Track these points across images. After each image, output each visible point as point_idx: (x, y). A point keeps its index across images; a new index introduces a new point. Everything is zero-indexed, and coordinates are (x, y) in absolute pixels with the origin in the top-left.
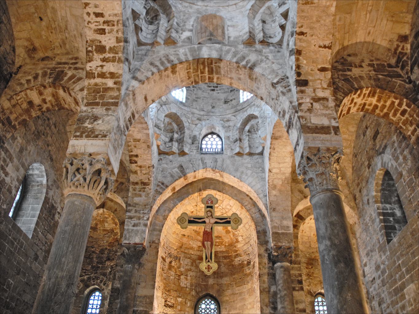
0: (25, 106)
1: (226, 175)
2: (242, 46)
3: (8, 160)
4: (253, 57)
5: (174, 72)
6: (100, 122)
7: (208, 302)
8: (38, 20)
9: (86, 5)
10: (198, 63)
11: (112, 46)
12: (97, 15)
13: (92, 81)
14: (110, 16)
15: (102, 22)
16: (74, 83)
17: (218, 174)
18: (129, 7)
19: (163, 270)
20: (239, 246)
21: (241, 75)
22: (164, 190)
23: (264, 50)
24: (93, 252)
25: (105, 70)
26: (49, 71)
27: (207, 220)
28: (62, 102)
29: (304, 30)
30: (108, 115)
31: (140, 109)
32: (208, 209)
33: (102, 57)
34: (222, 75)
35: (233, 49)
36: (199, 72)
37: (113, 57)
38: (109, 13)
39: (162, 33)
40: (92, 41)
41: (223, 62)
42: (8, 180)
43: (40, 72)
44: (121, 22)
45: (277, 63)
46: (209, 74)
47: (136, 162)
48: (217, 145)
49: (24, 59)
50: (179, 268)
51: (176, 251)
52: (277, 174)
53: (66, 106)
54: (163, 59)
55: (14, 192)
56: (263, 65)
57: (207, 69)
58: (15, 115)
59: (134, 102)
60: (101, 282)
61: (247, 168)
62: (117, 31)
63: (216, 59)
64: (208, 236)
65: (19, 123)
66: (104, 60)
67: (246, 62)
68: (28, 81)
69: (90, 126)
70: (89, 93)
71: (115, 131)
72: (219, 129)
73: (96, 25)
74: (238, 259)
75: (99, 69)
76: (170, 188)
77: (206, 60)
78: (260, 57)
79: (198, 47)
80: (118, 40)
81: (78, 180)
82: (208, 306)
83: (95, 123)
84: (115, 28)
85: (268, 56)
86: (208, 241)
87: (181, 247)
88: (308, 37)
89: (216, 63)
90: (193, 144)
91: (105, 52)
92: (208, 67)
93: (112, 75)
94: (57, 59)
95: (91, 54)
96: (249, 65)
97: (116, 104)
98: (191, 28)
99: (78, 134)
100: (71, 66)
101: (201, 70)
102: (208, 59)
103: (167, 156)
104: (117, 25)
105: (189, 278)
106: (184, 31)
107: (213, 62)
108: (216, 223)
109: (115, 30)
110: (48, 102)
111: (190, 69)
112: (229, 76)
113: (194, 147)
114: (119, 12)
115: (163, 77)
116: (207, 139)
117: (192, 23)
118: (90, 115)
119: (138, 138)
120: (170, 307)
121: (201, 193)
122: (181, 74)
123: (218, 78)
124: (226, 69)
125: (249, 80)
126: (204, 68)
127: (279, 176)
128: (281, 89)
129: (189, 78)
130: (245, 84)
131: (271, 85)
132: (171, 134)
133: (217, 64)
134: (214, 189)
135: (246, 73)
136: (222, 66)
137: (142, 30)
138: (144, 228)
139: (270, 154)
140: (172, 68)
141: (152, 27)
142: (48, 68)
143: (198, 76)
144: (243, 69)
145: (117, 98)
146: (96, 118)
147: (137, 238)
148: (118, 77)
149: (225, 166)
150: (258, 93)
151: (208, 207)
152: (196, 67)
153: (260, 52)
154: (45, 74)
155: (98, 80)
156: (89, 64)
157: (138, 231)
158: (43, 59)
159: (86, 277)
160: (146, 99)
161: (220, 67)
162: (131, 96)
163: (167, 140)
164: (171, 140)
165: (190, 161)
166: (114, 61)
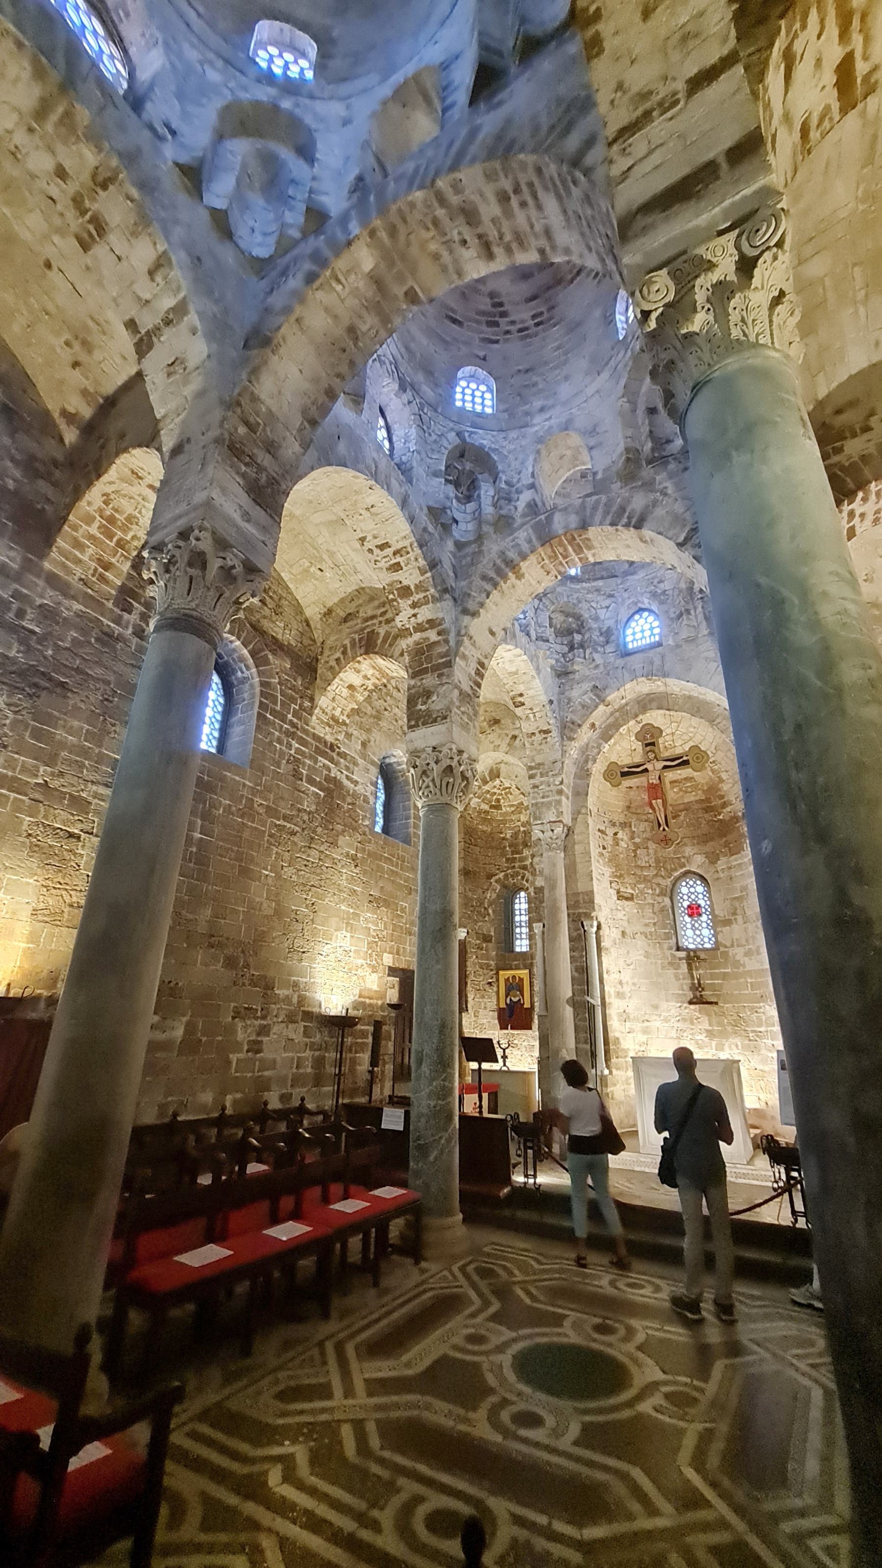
0: (345, 692)
1: (671, 681)
2: (619, 484)
3: (351, 766)
4: (638, 502)
6: (434, 698)
7: (691, 883)
8: (319, 572)
9: (362, 540)
12: (382, 547)
15: (391, 554)
16: (391, 645)
17: (659, 683)
18: (421, 509)
19: (604, 848)
20: (725, 787)
22: (576, 732)
23: (658, 478)
24: (504, 839)
25: (420, 619)
26: (356, 636)
27: (649, 766)
28: (388, 671)
30: (442, 684)
32: (648, 748)
33: (410, 602)
35: (604, 498)
36: (561, 558)
38: (395, 539)
39: (488, 510)
40: (390, 585)
42: (360, 789)
43: (347, 642)
45: (683, 499)
47: (523, 704)
48: (652, 629)
49: (323, 631)
50: (632, 838)
51: (622, 816)
53: (395, 674)
54: (499, 562)
55: (372, 800)
56: (659, 512)
57: (570, 549)
58: (339, 710)
60: (523, 878)
61: (706, 659)
62: (416, 559)
64: (656, 791)
65: (348, 716)
66: (414, 606)
67: (629, 518)
68: (338, 660)
69: (423, 708)
70: (412, 660)
71: (457, 704)
72: (646, 602)
74: (728, 809)
75: (413, 619)
76: (586, 727)
78: (652, 496)
79: (546, 518)
80: (423, 572)
81: (428, 787)
82: (692, 890)
83: (430, 701)
84: (412, 555)
85: (666, 488)
86: (656, 799)
87: (629, 807)
90: (607, 642)
91: (412, 594)
93: (432, 623)
94: (361, 614)
96: (633, 523)
97: (449, 664)
98: (531, 481)
99: (413, 723)
100: (381, 619)
103: (571, 676)
105: (651, 851)
106: (521, 492)
108: (665, 767)
113: (609, 649)
115: (506, 591)
116: (633, 624)
117: (530, 470)
118: (421, 690)
119: (514, 669)
120: (627, 899)
121: (638, 719)
125: (643, 545)
126: (566, 550)
128: (693, 553)
129: (548, 573)
132: (569, 638)
134: (660, 708)
137: (456, 522)
138: (557, 798)
141: (471, 507)
142: (355, 632)
143: (561, 563)
144: (626, 532)
145: (446, 655)
146: (427, 694)
147: (550, 813)
148: (440, 624)
151: (647, 745)
153: (649, 486)
154: (353, 643)
155: (417, 636)
157: (550, 803)
158: (345, 620)
159: (501, 875)
160: (492, 633)
161: (588, 539)
163: (566, 649)
164: (572, 648)
165: (608, 674)
166: (427, 603)
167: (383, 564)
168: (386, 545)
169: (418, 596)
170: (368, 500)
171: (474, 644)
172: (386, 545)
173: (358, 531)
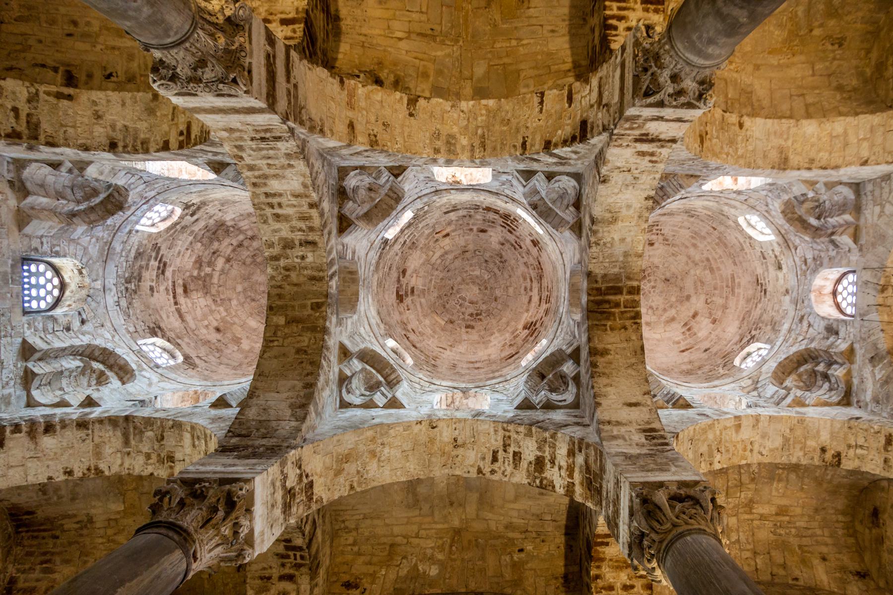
5: (605, 352)
10: (596, 312)
11: (536, 445)
12: (495, 459)
13: (578, 489)
14: (496, 440)
21: (613, 239)
25: (564, 464)
29: (519, 145)
31: (648, 416)
34: (622, 270)
37: (550, 447)
38: (493, 441)
40: (529, 474)
41: (592, 269)
44: (505, 425)
46: (621, 293)
52: (872, 145)
59: (626, 425)
62: (517, 433)
63: (589, 282)
66: (553, 462)
73: (509, 465)
77: (592, 298)
80: (529, 434)
84: (514, 435)
88: (528, 133)
89: (596, 282)
92: (605, 294)
93: (571, 453)
95: (545, 482)
101: (610, 308)
102: (589, 295)
104: (509, 431)
107: (595, 286)
109: (516, 436)
110: (631, 583)
111: (605, 325)
112: (621, 259)
114: (492, 425)
122: (612, 340)
123: (629, 278)
124: (607, 265)
125: (620, 224)
126: (608, 302)
127: (879, 140)
129: (625, 328)
130: (630, 231)
131: (607, 185)
133: (599, 279)
135: (605, 229)
136: (602, 272)
139: (825, 168)
140: (595, 354)
143: (622, 313)
144: (600, 235)
149: (876, 265)
150: (639, 205)
152: (605, 315)
156: (557, 488)
161: (605, 276)
162: (607, 427)
167: (509, 469)
168: (495, 453)
169: (547, 454)
170: (446, 440)
171: (618, 423)
172: (495, 453)
173: (471, 470)
